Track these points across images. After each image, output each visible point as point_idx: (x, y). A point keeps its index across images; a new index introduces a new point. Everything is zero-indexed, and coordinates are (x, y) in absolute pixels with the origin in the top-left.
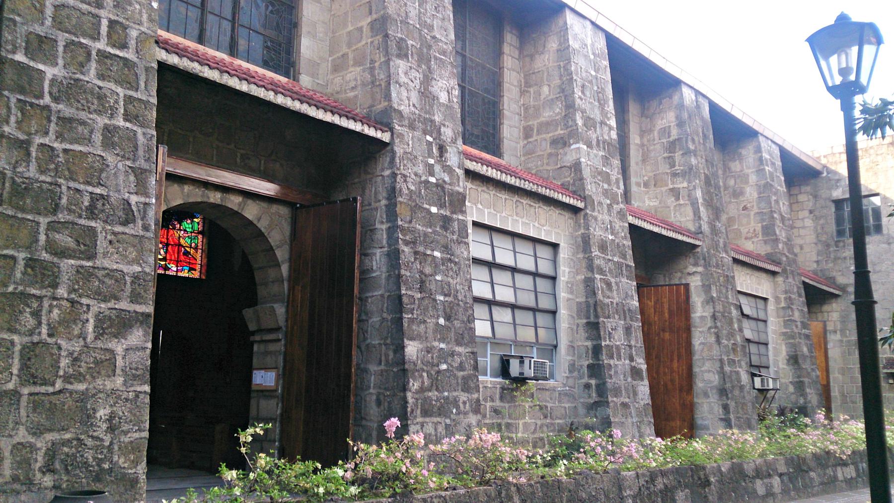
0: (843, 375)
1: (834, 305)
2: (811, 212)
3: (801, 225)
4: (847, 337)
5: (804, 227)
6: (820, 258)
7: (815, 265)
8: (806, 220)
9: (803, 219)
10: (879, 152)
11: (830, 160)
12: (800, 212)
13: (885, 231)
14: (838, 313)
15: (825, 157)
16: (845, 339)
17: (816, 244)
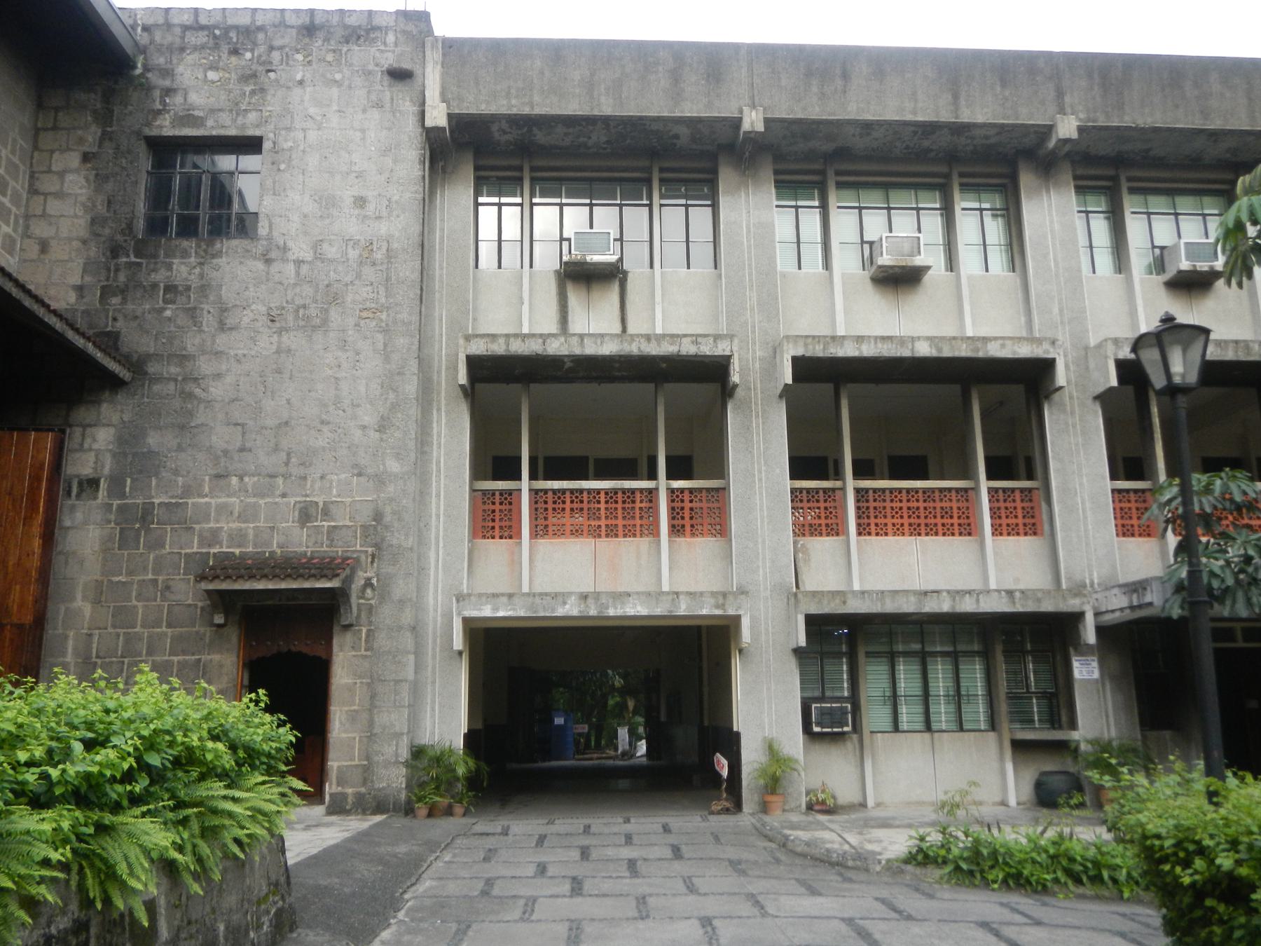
0: (97, 602)
1: (105, 408)
2: (86, 158)
3: (52, 189)
4: (123, 495)
5: (60, 195)
6: (88, 279)
7: (72, 297)
8: (70, 177)
9: (61, 174)
10: (277, 43)
11: (158, 37)
12: (56, 155)
13: (263, 230)
14: (112, 431)
15: (146, 29)
16: (116, 503)
17: (84, 242)
